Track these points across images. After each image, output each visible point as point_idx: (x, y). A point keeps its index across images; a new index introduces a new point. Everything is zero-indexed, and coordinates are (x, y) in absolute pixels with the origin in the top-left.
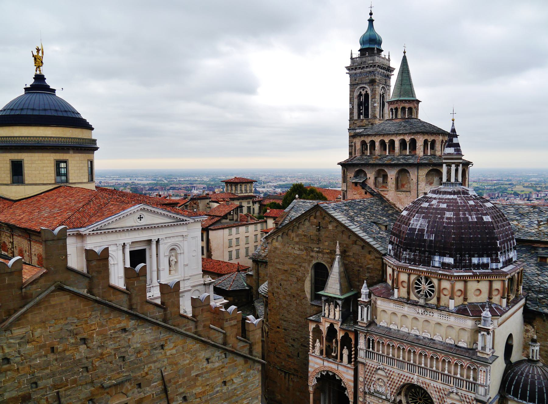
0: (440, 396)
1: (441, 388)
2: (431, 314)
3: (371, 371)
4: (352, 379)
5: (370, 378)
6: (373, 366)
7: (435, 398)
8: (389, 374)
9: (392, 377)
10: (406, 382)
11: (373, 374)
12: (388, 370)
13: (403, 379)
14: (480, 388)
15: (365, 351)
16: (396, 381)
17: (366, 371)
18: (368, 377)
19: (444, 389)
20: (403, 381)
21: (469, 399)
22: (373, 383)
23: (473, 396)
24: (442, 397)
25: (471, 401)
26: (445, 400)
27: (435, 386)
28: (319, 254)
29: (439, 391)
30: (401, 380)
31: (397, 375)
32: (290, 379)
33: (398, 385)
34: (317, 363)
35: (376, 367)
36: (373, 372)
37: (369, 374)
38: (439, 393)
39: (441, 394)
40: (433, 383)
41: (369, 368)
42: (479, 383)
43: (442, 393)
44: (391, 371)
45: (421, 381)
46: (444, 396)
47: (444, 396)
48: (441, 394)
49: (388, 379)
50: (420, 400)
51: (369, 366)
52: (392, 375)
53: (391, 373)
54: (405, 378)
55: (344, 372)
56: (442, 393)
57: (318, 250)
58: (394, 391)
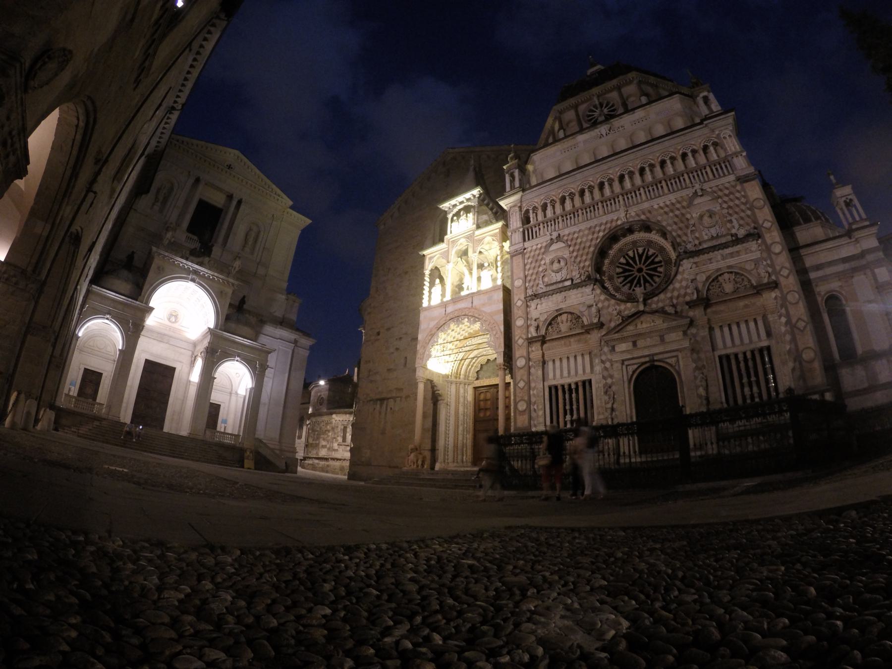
0: (677, 216)
1: (674, 201)
3: (536, 257)
4: (501, 306)
5: (535, 271)
6: (539, 246)
7: (671, 226)
8: (572, 240)
9: (579, 241)
10: (606, 232)
11: (542, 260)
12: (569, 235)
13: (599, 231)
14: (735, 160)
15: (521, 230)
16: (588, 244)
17: (525, 265)
18: (531, 272)
19: (680, 199)
20: (601, 234)
21: (727, 188)
22: (542, 274)
23: (732, 178)
24: (680, 216)
25: (732, 190)
26: (688, 216)
27: (662, 205)
29: (672, 207)
30: (595, 235)
31: (586, 232)
32: (389, 409)
33: (592, 249)
35: (544, 244)
36: (540, 257)
38: (672, 211)
39: (677, 212)
40: (657, 203)
41: (532, 254)
42: (730, 153)
43: (678, 209)
44: (574, 233)
45: (633, 214)
46: (684, 211)
47: (684, 211)
48: (677, 212)
49: (571, 249)
50: (640, 270)
51: (531, 251)
52: (577, 238)
53: (576, 235)
54: (603, 227)
56: (678, 209)
58: (587, 263)
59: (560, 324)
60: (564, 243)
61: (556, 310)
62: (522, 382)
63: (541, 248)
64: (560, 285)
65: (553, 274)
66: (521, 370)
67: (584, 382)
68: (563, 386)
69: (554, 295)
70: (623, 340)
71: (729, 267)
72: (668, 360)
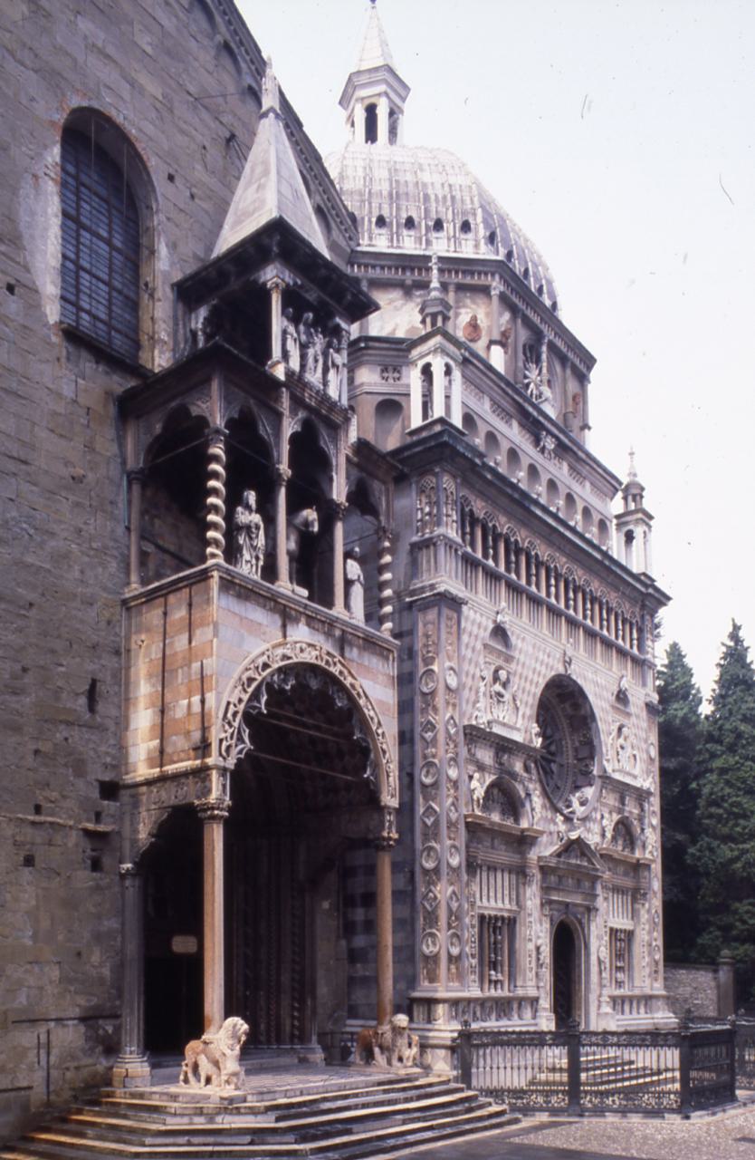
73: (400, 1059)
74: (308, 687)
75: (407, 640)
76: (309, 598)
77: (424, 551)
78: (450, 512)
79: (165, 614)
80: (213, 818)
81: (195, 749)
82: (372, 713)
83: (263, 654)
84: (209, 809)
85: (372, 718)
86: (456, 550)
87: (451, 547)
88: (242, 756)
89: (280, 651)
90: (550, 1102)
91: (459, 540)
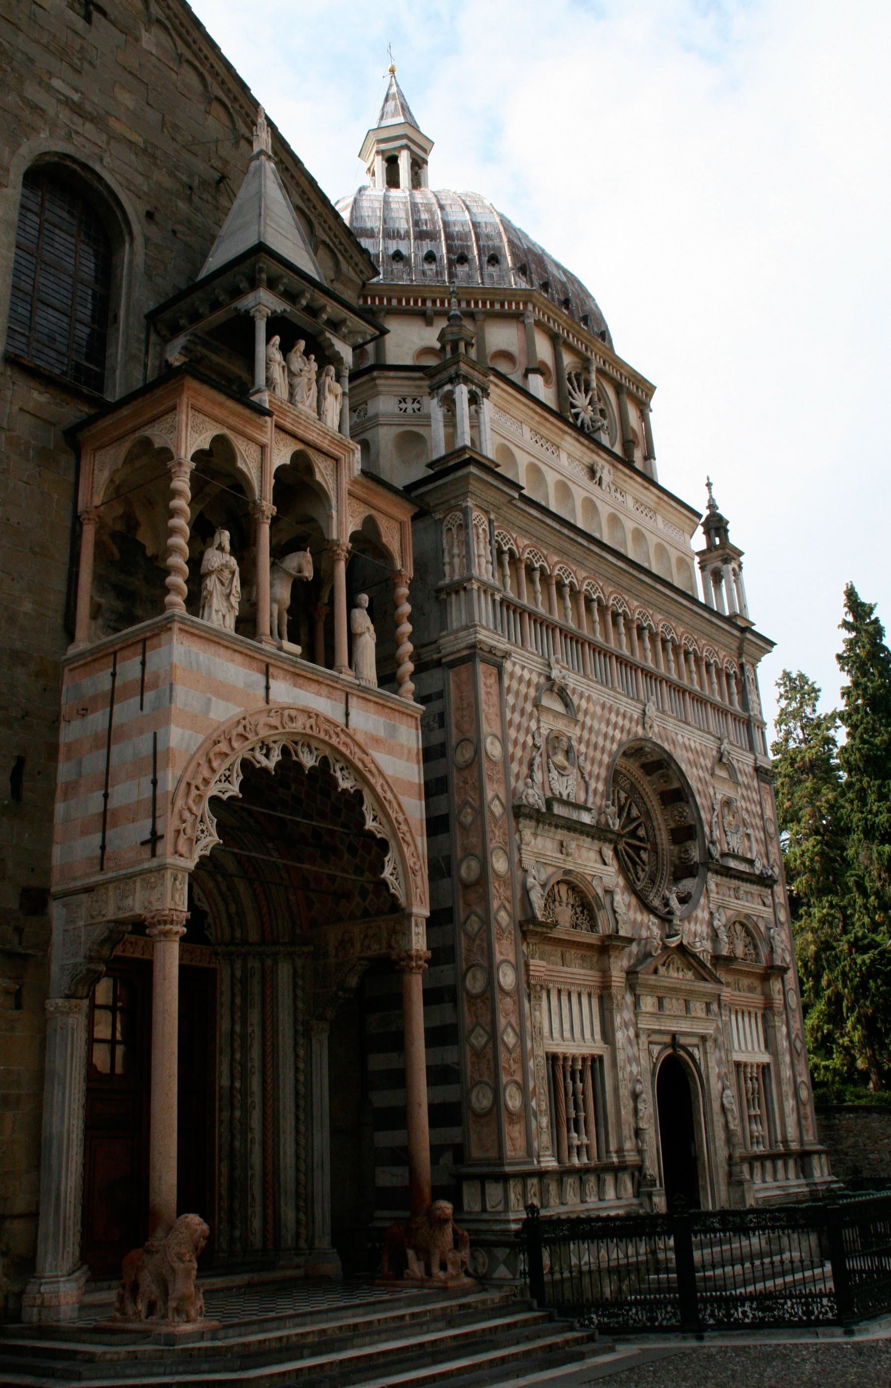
2: (618, 495)
11: (531, 716)
28: (76, 118)
31: (599, 710)
34: (225, 692)
35: (535, 679)
37: (517, 718)
55: (377, 741)
57: (76, 97)
59: (557, 904)
60: (566, 705)
61: (568, 872)
62: (509, 1030)
63: (529, 683)
64: (574, 815)
65: (554, 774)
66: (508, 999)
67: (593, 1058)
68: (565, 1059)
69: (559, 831)
70: (652, 989)
71: (748, 916)
72: (690, 1049)
73: (443, 1267)
74: (299, 765)
75: (436, 705)
76: (302, 656)
77: (453, 596)
78: (482, 552)
79: (114, 675)
80: (166, 934)
81: (143, 843)
82: (389, 796)
83: (238, 722)
84: (159, 922)
85: (390, 802)
86: (493, 595)
87: (485, 592)
88: (208, 853)
89: (263, 719)
90: (656, 1319)
91: (497, 584)
